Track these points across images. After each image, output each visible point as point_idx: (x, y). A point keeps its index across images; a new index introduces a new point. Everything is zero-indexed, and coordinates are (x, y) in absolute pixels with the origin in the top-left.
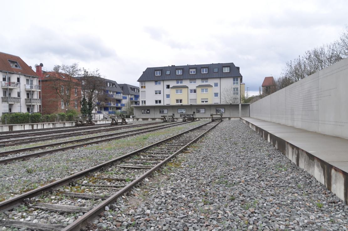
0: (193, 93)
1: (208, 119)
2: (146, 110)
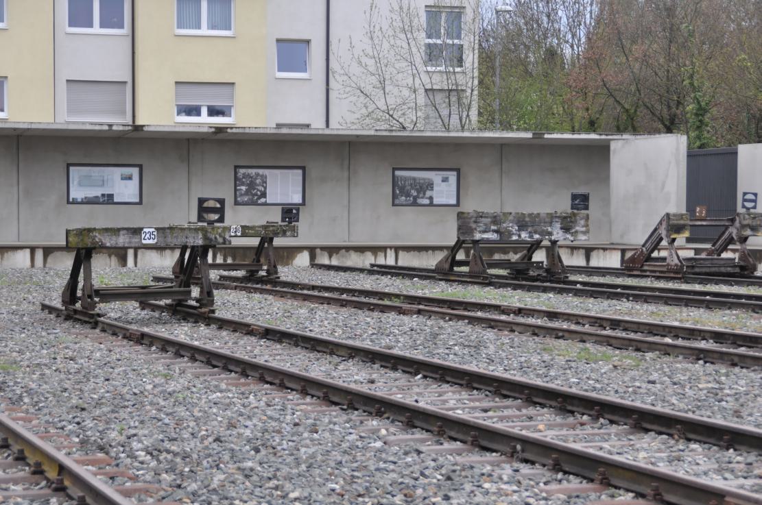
0: (96, 29)
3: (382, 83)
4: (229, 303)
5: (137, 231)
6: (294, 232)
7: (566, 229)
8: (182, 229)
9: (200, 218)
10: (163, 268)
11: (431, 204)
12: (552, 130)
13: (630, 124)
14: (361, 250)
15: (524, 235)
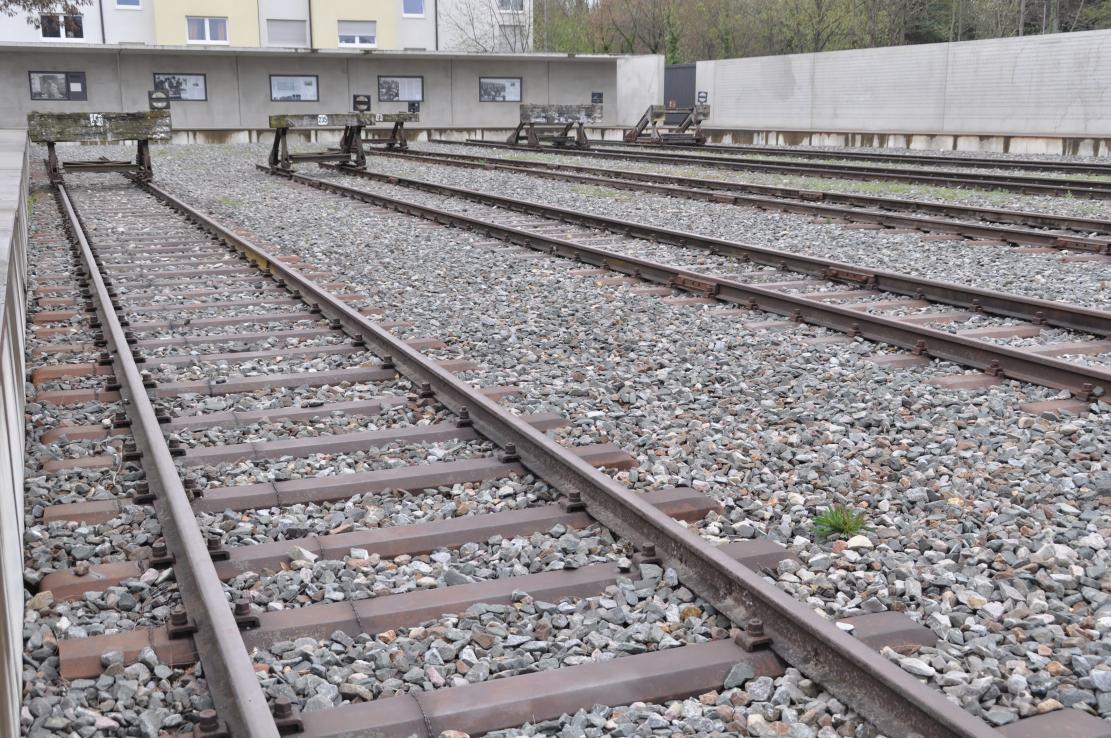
1: (479, 133)
2: (61, 77)
3: (472, 21)
4: (375, 164)
5: (315, 117)
6: (417, 118)
7: (589, 115)
8: (344, 115)
9: (355, 108)
10: (334, 143)
11: (504, 101)
12: (579, 52)
13: (630, 49)
14: (460, 130)
15: (562, 120)
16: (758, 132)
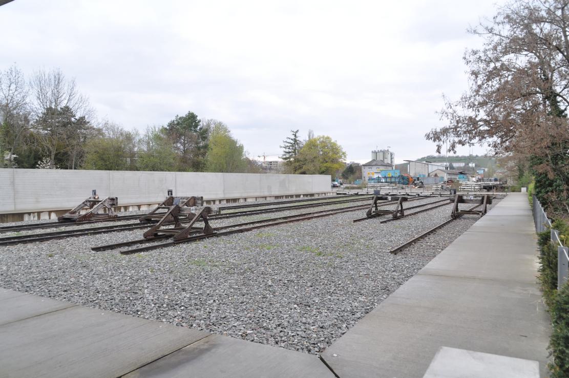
16: (29, 214)
